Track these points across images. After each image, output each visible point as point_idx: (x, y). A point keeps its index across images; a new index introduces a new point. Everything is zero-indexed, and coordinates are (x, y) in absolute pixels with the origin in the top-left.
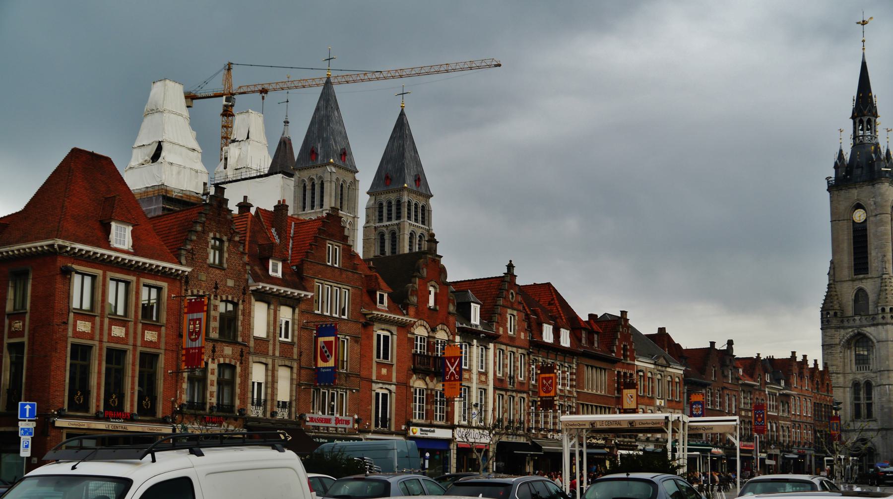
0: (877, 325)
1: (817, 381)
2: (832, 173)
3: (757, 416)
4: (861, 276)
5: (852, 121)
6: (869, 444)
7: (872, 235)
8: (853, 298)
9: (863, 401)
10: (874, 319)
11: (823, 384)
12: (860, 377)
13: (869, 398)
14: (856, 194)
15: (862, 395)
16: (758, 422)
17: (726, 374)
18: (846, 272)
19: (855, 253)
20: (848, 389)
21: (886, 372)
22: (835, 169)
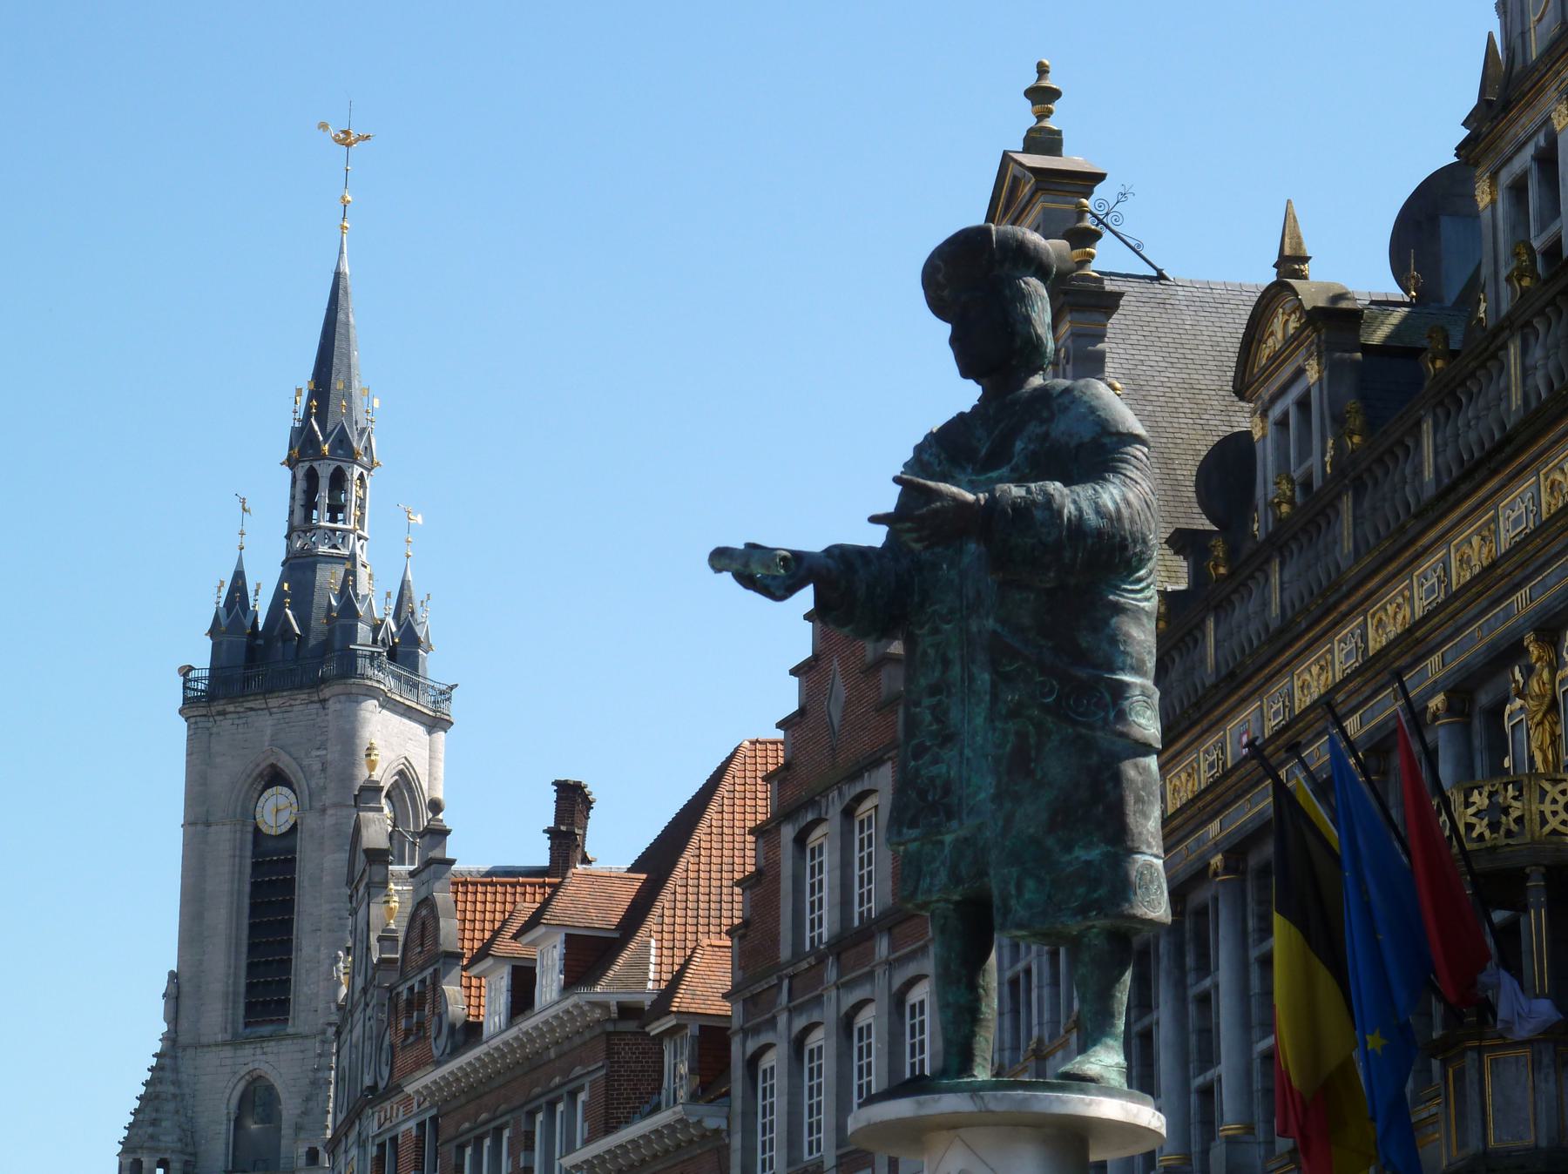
2: (201, 657)
5: (287, 473)
7: (306, 884)
14: (269, 732)
18: (216, 1016)
19: (253, 948)
22: (211, 637)
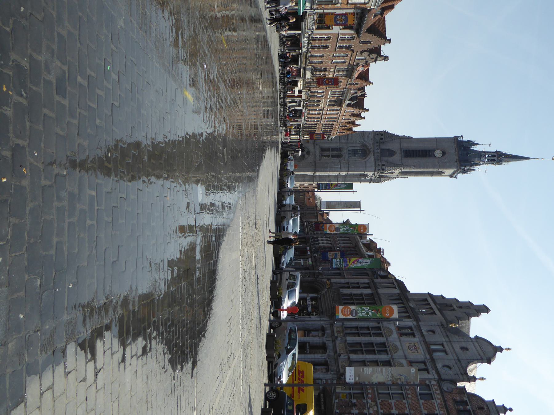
0: (375, 162)
1: (347, 126)
2: (465, 139)
3: (330, 80)
4: (403, 154)
5: (495, 151)
6: (306, 156)
8: (391, 149)
9: (331, 153)
10: (378, 160)
11: (344, 130)
12: (345, 152)
13: (333, 156)
15: (335, 153)
16: (326, 81)
17: (363, 54)
18: (405, 145)
20: (338, 145)
21: (348, 166)
